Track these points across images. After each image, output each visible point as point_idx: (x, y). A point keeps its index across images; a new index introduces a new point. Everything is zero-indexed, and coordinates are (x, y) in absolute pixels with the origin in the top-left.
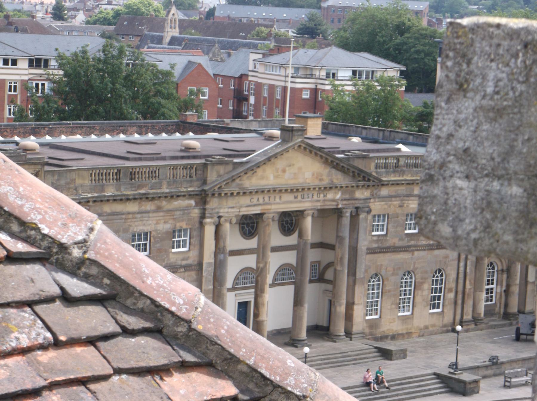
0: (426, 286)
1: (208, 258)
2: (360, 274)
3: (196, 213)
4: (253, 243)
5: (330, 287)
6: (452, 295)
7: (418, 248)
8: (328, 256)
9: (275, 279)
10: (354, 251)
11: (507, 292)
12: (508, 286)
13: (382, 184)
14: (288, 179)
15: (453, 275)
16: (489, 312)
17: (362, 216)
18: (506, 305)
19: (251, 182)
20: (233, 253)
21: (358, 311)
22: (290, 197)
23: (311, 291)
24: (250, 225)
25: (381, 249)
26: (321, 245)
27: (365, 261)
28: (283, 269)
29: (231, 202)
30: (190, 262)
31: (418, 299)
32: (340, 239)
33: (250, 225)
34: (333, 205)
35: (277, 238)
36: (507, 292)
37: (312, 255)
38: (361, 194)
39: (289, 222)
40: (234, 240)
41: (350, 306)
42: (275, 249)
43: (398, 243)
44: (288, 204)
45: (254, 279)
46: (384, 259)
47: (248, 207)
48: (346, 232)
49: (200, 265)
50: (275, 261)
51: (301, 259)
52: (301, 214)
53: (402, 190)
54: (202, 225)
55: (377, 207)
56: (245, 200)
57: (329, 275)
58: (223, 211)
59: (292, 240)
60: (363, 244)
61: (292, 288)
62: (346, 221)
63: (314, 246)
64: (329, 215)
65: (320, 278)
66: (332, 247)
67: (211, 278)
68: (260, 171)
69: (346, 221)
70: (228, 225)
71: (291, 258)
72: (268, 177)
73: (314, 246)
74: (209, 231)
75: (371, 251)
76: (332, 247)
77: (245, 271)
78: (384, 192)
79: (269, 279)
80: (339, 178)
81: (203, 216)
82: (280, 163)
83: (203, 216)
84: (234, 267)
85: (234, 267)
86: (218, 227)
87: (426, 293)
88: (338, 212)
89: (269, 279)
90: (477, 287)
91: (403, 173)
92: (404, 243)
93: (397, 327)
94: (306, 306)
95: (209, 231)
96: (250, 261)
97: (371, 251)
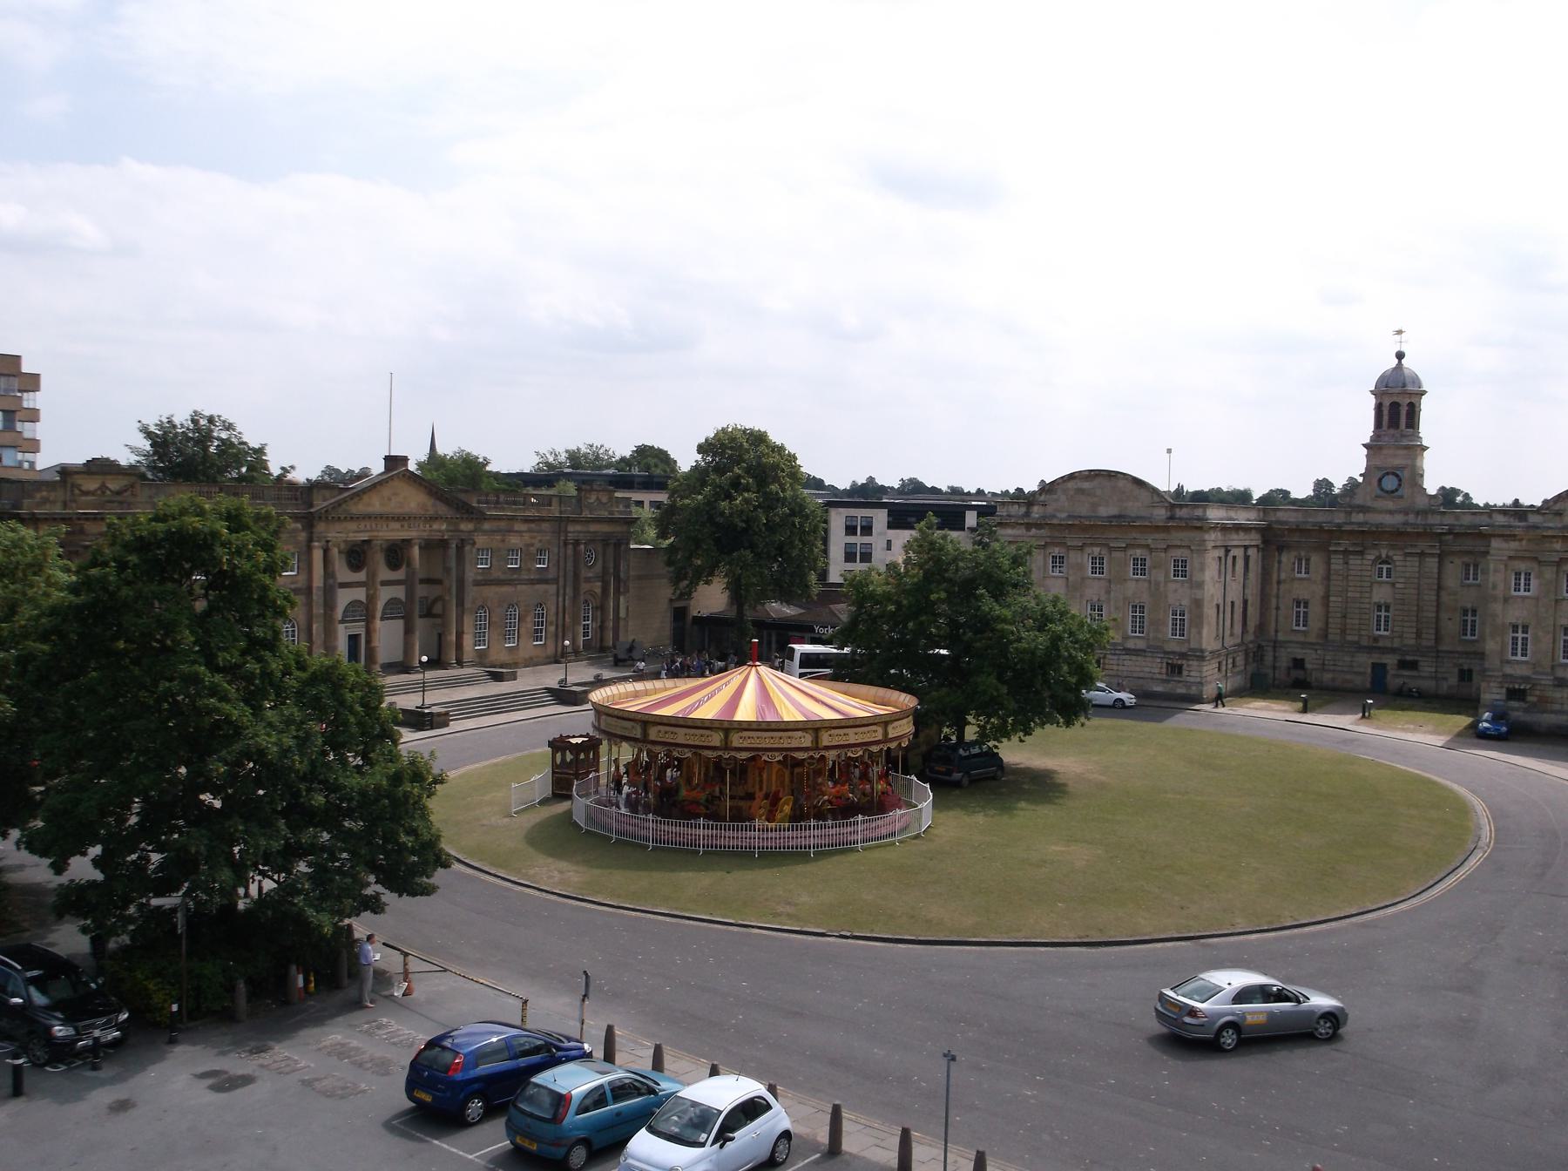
0: (529, 619)
1: (318, 582)
2: (468, 605)
3: (303, 536)
4: (361, 576)
5: (438, 621)
6: (552, 629)
7: (521, 582)
8: (436, 591)
9: (384, 613)
10: (461, 583)
11: (602, 628)
12: (603, 622)
13: (482, 517)
14: (392, 507)
15: (553, 609)
16: (587, 645)
17: (467, 548)
18: (602, 640)
19: (359, 508)
20: (344, 585)
21: (468, 640)
22: (396, 525)
23: (420, 624)
24: (357, 556)
25: (486, 581)
26: (428, 581)
27: (472, 592)
28: (392, 602)
29: (338, 526)
30: (299, 585)
31: (523, 631)
32: (447, 570)
33: (357, 556)
34: (437, 536)
35: (384, 573)
36: (602, 628)
37: (421, 591)
38: (466, 526)
39: (396, 554)
40: (343, 573)
41: (460, 635)
42: (384, 583)
43: (503, 577)
44: (395, 532)
45: (364, 612)
46: (490, 592)
47: (356, 533)
48: (453, 564)
49: (309, 590)
50: (384, 595)
51: (410, 593)
52: (407, 543)
53: (503, 525)
54: (309, 549)
55: (481, 540)
56: (352, 526)
57: (437, 609)
58: (331, 535)
59: (400, 574)
60: (470, 576)
61: (401, 622)
62: (452, 551)
63: (422, 581)
64: (434, 547)
65: (428, 614)
66: (439, 582)
67: (321, 601)
68: (365, 497)
69: (452, 551)
70: (336, 550)
71: (399, 592)
72: (375, 504)
73: (422, 581)
74: (318, 555)
75: (477, 583)
76: (439, 582)
77: (354, 604)
78: (487, 526)
79: (379, 614)
80: (443, 509)
81: (310, 540)
82: (386, 491)
83: (310, 540)
84: (344, 598)
85: (344, 598)
86: (326, 551)
87: (530, 625)
88: (443, 544)
89: (379, 614)
90: (576, 621)
91: (503, 509)
92: (508, 576)
93: (504, 657)
94: (417, 634)
95: (318, 555)
96: (360, 594)
97: (477, 583)
